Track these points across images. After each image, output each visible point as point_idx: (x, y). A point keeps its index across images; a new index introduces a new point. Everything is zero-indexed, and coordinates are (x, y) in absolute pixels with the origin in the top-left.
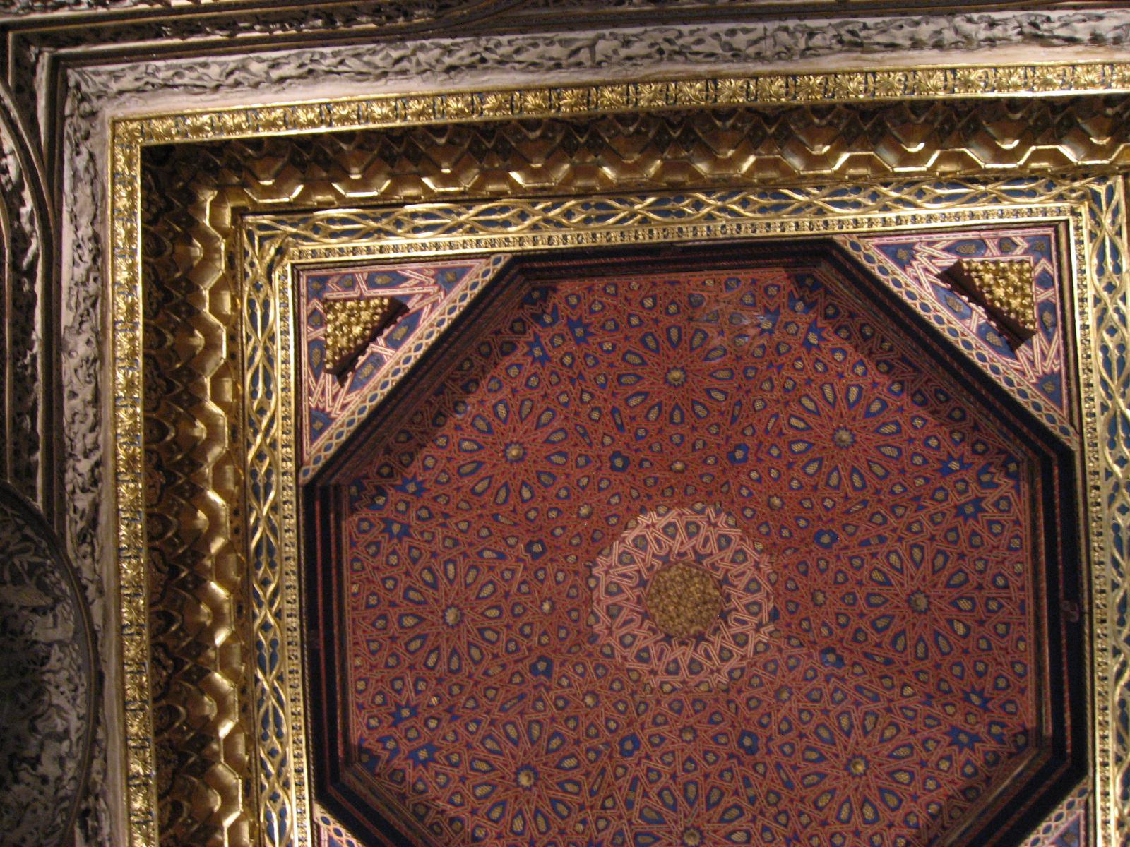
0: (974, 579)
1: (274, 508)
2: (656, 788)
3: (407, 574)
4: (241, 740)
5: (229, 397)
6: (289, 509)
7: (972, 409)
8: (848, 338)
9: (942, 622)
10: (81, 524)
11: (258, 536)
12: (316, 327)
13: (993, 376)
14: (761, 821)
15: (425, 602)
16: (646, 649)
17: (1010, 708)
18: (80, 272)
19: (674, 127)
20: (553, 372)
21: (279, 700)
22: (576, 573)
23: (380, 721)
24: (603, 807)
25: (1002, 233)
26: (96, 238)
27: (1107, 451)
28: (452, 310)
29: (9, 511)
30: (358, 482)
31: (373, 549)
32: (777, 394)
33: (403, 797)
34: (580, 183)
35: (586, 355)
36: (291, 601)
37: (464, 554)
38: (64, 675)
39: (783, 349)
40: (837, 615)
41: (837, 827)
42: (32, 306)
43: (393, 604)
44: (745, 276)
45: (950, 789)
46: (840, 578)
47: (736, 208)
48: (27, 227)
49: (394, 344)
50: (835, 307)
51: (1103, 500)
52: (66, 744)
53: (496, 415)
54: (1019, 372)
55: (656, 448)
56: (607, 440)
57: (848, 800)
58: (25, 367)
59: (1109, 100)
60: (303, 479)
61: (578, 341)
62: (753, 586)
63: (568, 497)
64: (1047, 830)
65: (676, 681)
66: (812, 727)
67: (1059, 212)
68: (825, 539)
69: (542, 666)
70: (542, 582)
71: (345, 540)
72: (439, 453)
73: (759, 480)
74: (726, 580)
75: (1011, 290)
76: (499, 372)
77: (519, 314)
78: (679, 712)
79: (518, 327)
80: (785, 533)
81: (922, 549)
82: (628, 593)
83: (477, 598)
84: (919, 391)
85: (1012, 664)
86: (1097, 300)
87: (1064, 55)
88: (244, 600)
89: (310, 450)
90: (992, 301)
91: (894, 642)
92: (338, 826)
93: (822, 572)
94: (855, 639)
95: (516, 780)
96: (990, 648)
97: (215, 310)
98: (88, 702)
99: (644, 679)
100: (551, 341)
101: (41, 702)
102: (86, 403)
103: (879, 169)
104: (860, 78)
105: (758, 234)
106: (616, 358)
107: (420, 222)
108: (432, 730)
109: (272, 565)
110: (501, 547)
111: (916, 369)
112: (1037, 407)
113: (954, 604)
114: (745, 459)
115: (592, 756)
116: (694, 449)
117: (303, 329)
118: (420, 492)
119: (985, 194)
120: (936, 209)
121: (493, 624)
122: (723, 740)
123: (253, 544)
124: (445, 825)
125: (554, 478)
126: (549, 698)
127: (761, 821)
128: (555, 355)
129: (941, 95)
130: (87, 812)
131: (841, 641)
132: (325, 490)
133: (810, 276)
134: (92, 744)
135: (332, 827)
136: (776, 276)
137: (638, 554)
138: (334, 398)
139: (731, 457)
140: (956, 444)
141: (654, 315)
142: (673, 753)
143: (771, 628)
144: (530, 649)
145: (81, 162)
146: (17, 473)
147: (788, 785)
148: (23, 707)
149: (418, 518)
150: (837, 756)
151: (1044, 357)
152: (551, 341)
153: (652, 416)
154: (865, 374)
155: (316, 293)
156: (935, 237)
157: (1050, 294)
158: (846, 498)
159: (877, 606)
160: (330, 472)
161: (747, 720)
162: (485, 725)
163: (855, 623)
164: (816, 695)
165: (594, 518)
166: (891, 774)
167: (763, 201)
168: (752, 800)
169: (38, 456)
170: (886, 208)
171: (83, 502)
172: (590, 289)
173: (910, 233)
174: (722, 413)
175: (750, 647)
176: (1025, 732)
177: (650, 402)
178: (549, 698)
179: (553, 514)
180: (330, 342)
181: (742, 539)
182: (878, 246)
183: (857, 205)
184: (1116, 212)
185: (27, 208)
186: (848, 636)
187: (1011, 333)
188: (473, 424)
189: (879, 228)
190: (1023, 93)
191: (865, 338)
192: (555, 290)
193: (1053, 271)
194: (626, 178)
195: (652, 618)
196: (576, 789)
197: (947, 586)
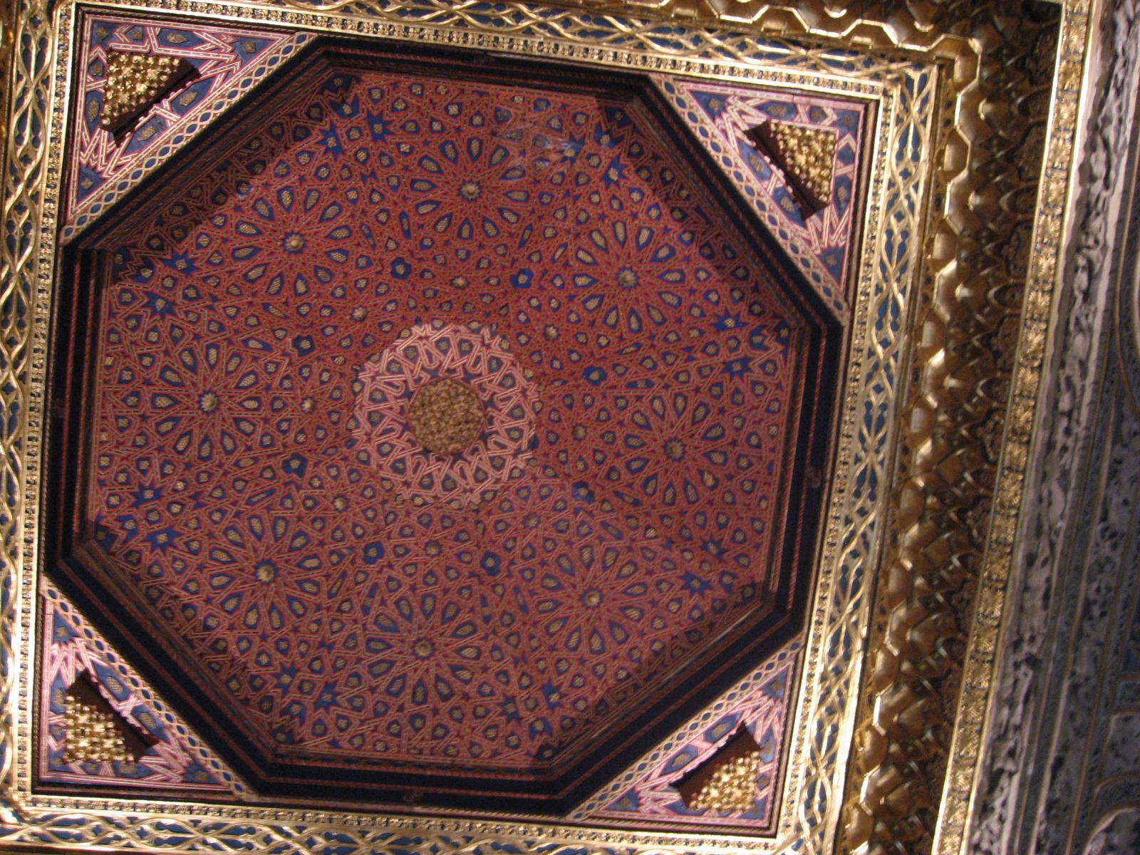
0: (731, 435)
1: (29, 265)
2: (394, 598)
3: (166, 353)
6: (46, 268)
7: (755, 268)
8: (648, 180)
9: (694, 472)
11: (8, 292)
12: (96, 78)
13: (781, 241)
14: (493, 640)
15: (181, 385)
16: (402, 460)
17: (744, 561)
20: (344, 166)
21: (14, 466)
22: (342, 375)
23: (121, 500)
24: (340, 610)
25: (815, 102)
27: (874, 330)
28: (246, 84)
30: (124, 250)
31: (133, 322)
32: (569, 224)
35: (382, 154)
39: (582, 180)
40: (595, 451)
41: (564, 654)
43: (147, 382)
44: (557, 99)
45: (675, 630)
46: (603, 416)
47: (556, 26)
49: (180, 109)
50: (641, 146)
53: (280, 200)
54: (805, 241)
55: (440, 260)
56: (392, 245)
57: (578, 629)
61: (376, 137)
62: (517, 412)
63: (343, 297)
64: (758, 676)
65: (428, 495)
66: (554, 555)
67: (873, 90)
69: (295, 464)
70: (306, 379)
71: (104, 310)
73: (539, 308)
74: (490, 403)
75: (812, 159)
76: (289, 157)
77: (318, 99)
78: (427, 525)
79: (315, 112)
80: (557, 364)
81: (686, 399)
82: (392, 402)
83: (237, 387)
84: (707, 244)
85: (753, 520)
86: (891, 184)
89: (76, 209)
90: (793, 166)
91: (645, 485)
92: (65, 601)
93: (587, 407)
94: (608, 477)
95: (254, 574)
96: (734, 503)
99: (397, 489)
100: (348, 133)
105: (574, 57)
106: (412, 162)
108: (175, 515)
109: (21, 325)
110: (269, 339)
111: (708, 222)
112: (816, 278)
113: (707, 455)
114: (528, 285)
115: (335, 558)
116: (478, 267)
117: (83, 77)
118: (188, 271)
119: (805, 59)
120: (755, 65)
121: (249, 415)
122: (467, 558)
124: (177, 611)
125: (332, 275)
126: (299, 496)
128: (350, 148)
131: (595, 476)
132: (87, 254)
133: (621, 110)
135: (58, 601)
136: (586, 104)
138: (108, 157)
140: (735, 302)
142: (416, 564)
143: (528, 455)
144: (285, 446)
147: (524, 609)
149: (185, 296)
150: (574, 586)
151: (832, 231)
152: (348, 133)
153: (441, 227)
154: (659, 217)
155: (103, 42)
156: (749, 93)
157: (849, 170)
158: (621, 338)
159: (634, 448)
160: (95, 236)
161: (493, 542)
162: (229, 516)
163: (610, 461)
164: (562, 526)
165: (368, 322)
167: (585, 25)
168: (487, 619)
170: (706, 55)
172: (395, 86)
173: (726, 84)
174: (511, 235)
175: (505, 473)
176: (753, 585)
178: (299, 496)
179: (326, 312)
180: (109, 95)
181: (513, 364)
182: (692, 92)
183: (678, 46)
184: (925, 101)
186: (602, 474)
187: (805, 201)
188: (254, 207)
189: (695, 73)
191: (665, 183)
192: (359, 81)
193: (856, 147)
195: (412, 430)
196: (314, 589)
197: (704, 438)
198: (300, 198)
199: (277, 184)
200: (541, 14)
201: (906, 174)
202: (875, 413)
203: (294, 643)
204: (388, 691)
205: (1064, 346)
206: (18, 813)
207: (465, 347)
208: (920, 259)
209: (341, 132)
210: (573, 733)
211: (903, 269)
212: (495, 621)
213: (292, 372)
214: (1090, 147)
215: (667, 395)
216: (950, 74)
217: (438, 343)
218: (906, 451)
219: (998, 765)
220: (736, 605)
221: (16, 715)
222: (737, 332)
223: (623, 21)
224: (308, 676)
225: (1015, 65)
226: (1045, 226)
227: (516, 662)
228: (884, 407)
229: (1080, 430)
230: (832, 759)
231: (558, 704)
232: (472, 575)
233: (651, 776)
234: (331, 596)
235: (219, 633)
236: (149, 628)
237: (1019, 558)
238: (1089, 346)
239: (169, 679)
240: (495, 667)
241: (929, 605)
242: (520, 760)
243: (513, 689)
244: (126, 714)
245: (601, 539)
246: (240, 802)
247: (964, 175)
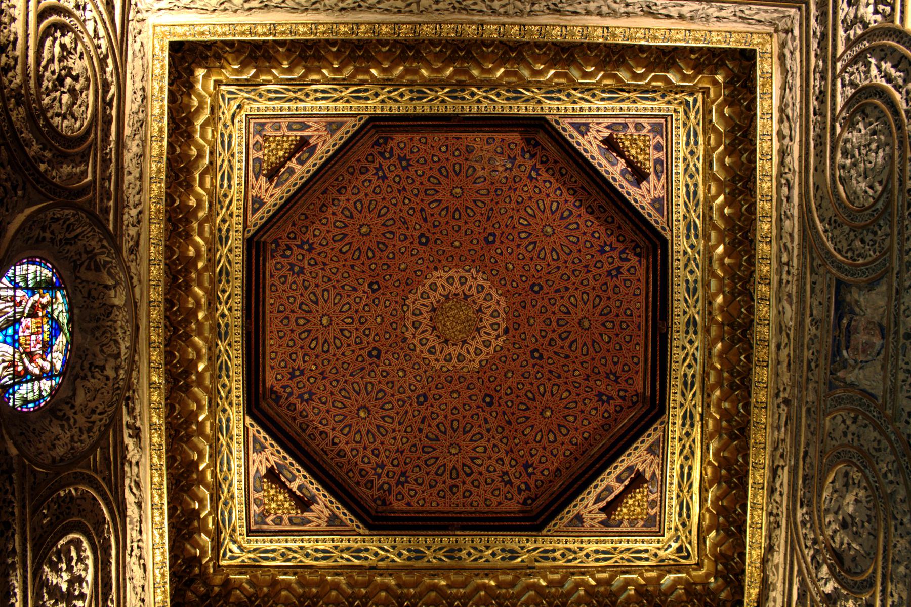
1: (230, 250)
2: (435, 423)
3: (302, 295)
4: (207, 375)
5: (208, 185)
6: (239, 252)
7: (618, 219)
10: (131, 243)
12: (257, 151)
15: (310, 312)
16: (434, 347)
17: (630, 381)
18: (135, 107)
19: (461, 50)
21: (229, 356)
26: (143, 89)
28: (334, 145)
30: (276, 241)
31: (283, 280)
32: (513, 204)
33: (294, 419)
34: (408, 78)
35: (408, 177)
36: (237, 302)
37: (334, 286)
39: (517, 179)
42: (110, 122)
43: (293, 311)
45: (595, 425)
46: (543, 310)
47: (494, 97)
48: (110, 79)
49: (301, 162)
51: (681, 267)
53: (356, 207)
54: (642, 196)
55: (445, 233)
56: (417, 227)
59: (692, 50)
60: (247, 235)
61: (404, 169)
62: (495, 314)
63: (394, 258)
64: (643, 442)
66: (523, 392)
67: (668, 110)
68: (536, 288)
69: (375, 353)
72: (323, 228)
73: (501, 254)
74: (480, 310)
77: (371, 151)
79: (370, 158)
80: (515, 284)
82: (425, 315)
86: (685, 159)
87: (665, 24)
88: (213, 301)
89: (252, 219)
91: (570, 346)
94: (550, 344)
97: (203, 137)
98: (131, 340)
99: (432, 364)
102: (136, 179)
103: (571, 80)
104: (558, 29)
106: (424, 179)
107: (319, 95)
109: (228, 282)
110: (355, 284)
111: (589, 193)
115: (401, 403)
118: (310, 250)
119: (628, 98)
120: (602, 104)
121: (348, 327)
123: (218, 270)
124: (317, 435)
127: (493, 442)
129: (601, 40)
130: (128, 398)
132: (258, 243)
134: (132, 362)
136: (515, 137)
137: (432, 294)
139: (486, 240)
140: (609, 236)
141: (446, 156)
143: (504, 338)
145: (137, 46)
146: (101, 210)
147: (509, 423)
151: (656, 189)
153: (443, 214)
156: (601, 120)
157: (661, 155)
158: (549, 265)
162: (341, 383)
164: (527, 375)
166: (565, 417)
167: (508, 95)
168: (488, 431)
169: (111, 203)
170: (575, 102)
171: (132, 231)
172: (411, 139)
173: (587, 116)
175: (492, 348)
176: (637, 395)
177: (442, 206)
179: (385, 267)
183: (559, 99)
184: (697, 112)
185: (110, 68)
189: (570, 112)
190: (643, 42)
191: (562, 175)
194: (433, 76)
197: (601, 315)
198: (366, 205)
199: (354, 199)
200: (485, 91)
201: (692, 153)
202: (692, 286)
203: (382, 451)
204: (436, 474)
205: (780, 228)
206: (240, 547)
207: (463, 280)
208: (705, 197)
209: (385, 167)
210: (542, 489)
211: (697, 205)
212: (493, 432)
213: (370, 301)
214: (781, 121)
215: (577, 294)
216: (708, 97)
217: (447, 279)
218: (710, 303)
219: (776, 463)
220: (629, 407)
221: (237, 492)
222: (612, 253)
223: (528, 90)
224: (391, 468)
225: (741, 86)
226: (763, 167)
227: (507, 453)
228: (696, 281)
229: (794, 271)
230: (691, 486)
231: (534, 474)
232: (478, 407)
233: (588, 504)
234: (400, 424)
235: (342, 446)
236: (303, 444)
237: (773, 346)
238: (792, 225)
239: (316, 470)
240: (496, 456)
241: (732, 387)
242: (513, 506)
243: (507, 468)
244: (295, 489)
245: (549, 379)
246: (360, 535)
247: (722, 148)
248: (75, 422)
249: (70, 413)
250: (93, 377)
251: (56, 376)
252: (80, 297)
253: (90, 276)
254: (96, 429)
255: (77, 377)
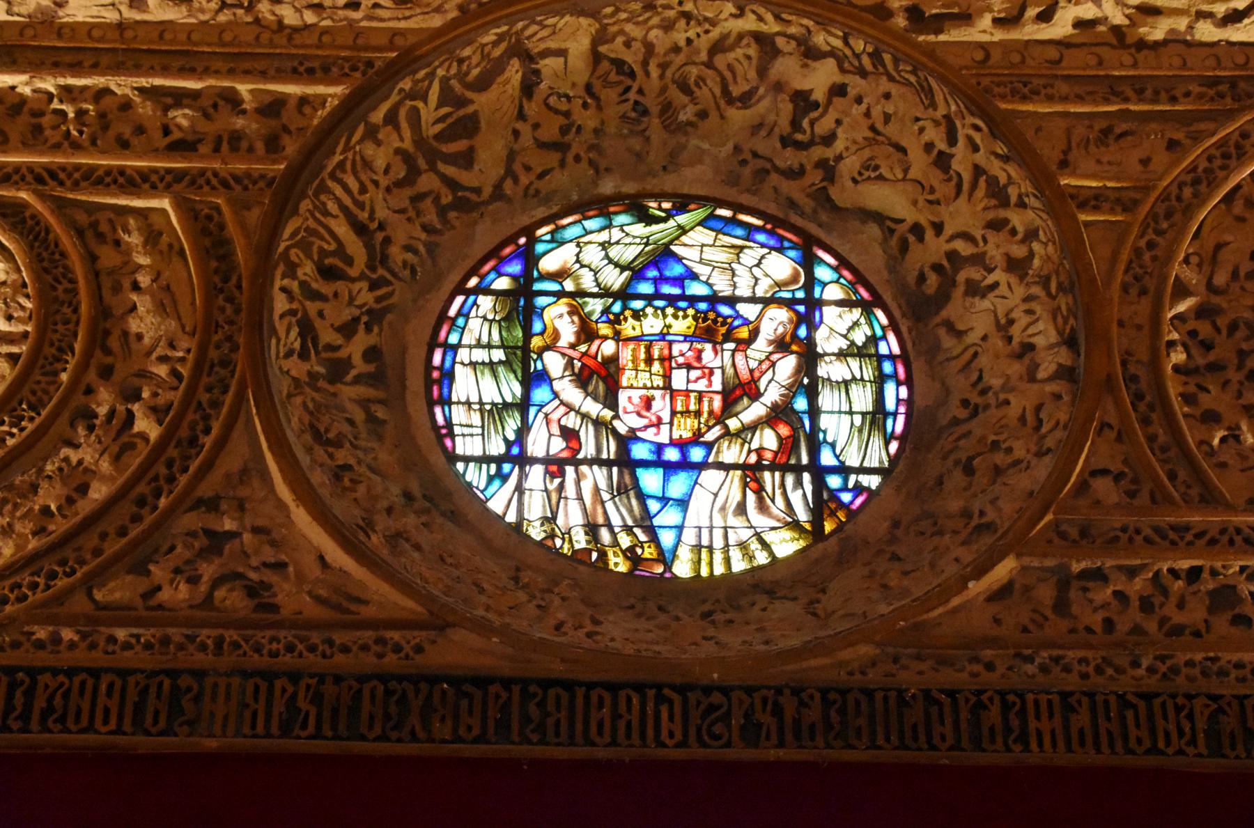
29: (338, 158)
38: (654, 34)
52: (780, 42)
58: (80, 113)
101: (701, 80)
148: (703, 115)
169: (244, 88)
248: (967, 237)
249: (935, 248)
250: (829, 139)
251: (811, 281)
252: (560, 179)
253: (490, 153)
254: (996, 169)
255: (822, 198)
